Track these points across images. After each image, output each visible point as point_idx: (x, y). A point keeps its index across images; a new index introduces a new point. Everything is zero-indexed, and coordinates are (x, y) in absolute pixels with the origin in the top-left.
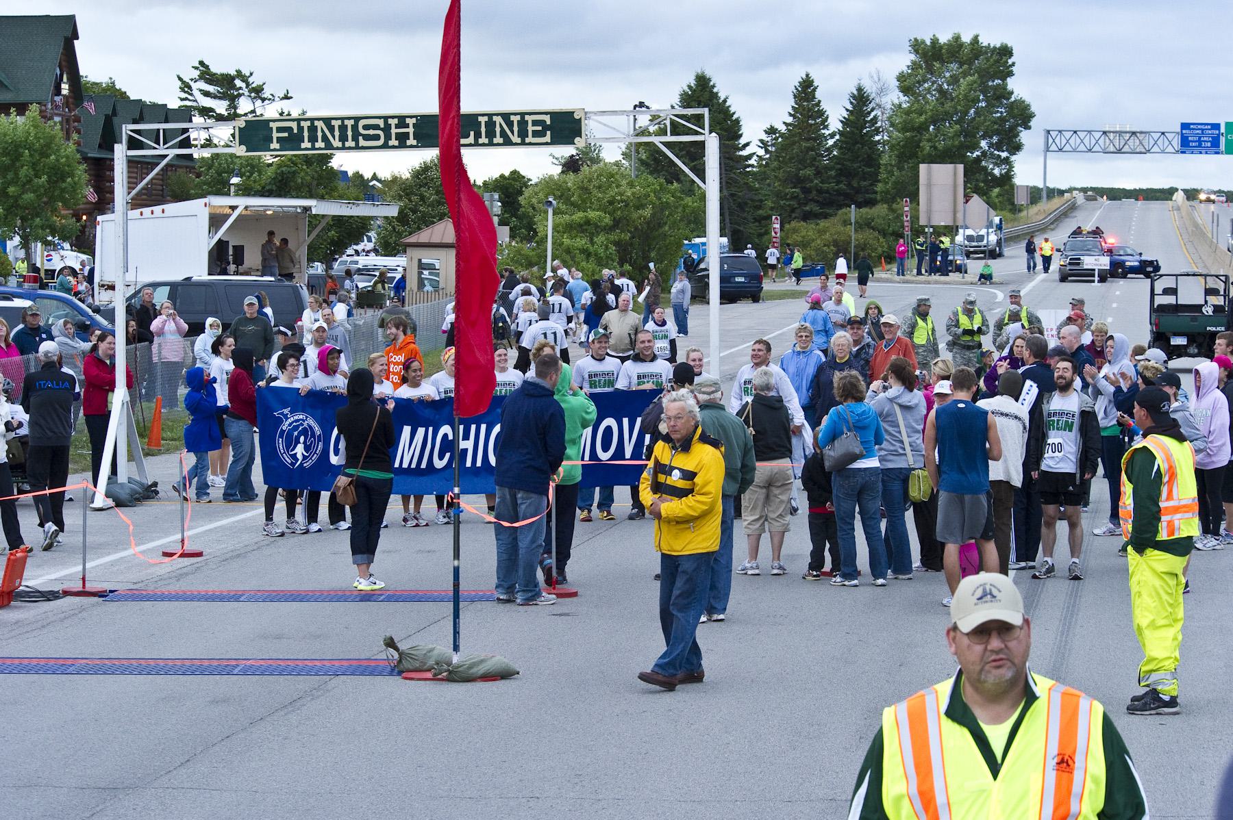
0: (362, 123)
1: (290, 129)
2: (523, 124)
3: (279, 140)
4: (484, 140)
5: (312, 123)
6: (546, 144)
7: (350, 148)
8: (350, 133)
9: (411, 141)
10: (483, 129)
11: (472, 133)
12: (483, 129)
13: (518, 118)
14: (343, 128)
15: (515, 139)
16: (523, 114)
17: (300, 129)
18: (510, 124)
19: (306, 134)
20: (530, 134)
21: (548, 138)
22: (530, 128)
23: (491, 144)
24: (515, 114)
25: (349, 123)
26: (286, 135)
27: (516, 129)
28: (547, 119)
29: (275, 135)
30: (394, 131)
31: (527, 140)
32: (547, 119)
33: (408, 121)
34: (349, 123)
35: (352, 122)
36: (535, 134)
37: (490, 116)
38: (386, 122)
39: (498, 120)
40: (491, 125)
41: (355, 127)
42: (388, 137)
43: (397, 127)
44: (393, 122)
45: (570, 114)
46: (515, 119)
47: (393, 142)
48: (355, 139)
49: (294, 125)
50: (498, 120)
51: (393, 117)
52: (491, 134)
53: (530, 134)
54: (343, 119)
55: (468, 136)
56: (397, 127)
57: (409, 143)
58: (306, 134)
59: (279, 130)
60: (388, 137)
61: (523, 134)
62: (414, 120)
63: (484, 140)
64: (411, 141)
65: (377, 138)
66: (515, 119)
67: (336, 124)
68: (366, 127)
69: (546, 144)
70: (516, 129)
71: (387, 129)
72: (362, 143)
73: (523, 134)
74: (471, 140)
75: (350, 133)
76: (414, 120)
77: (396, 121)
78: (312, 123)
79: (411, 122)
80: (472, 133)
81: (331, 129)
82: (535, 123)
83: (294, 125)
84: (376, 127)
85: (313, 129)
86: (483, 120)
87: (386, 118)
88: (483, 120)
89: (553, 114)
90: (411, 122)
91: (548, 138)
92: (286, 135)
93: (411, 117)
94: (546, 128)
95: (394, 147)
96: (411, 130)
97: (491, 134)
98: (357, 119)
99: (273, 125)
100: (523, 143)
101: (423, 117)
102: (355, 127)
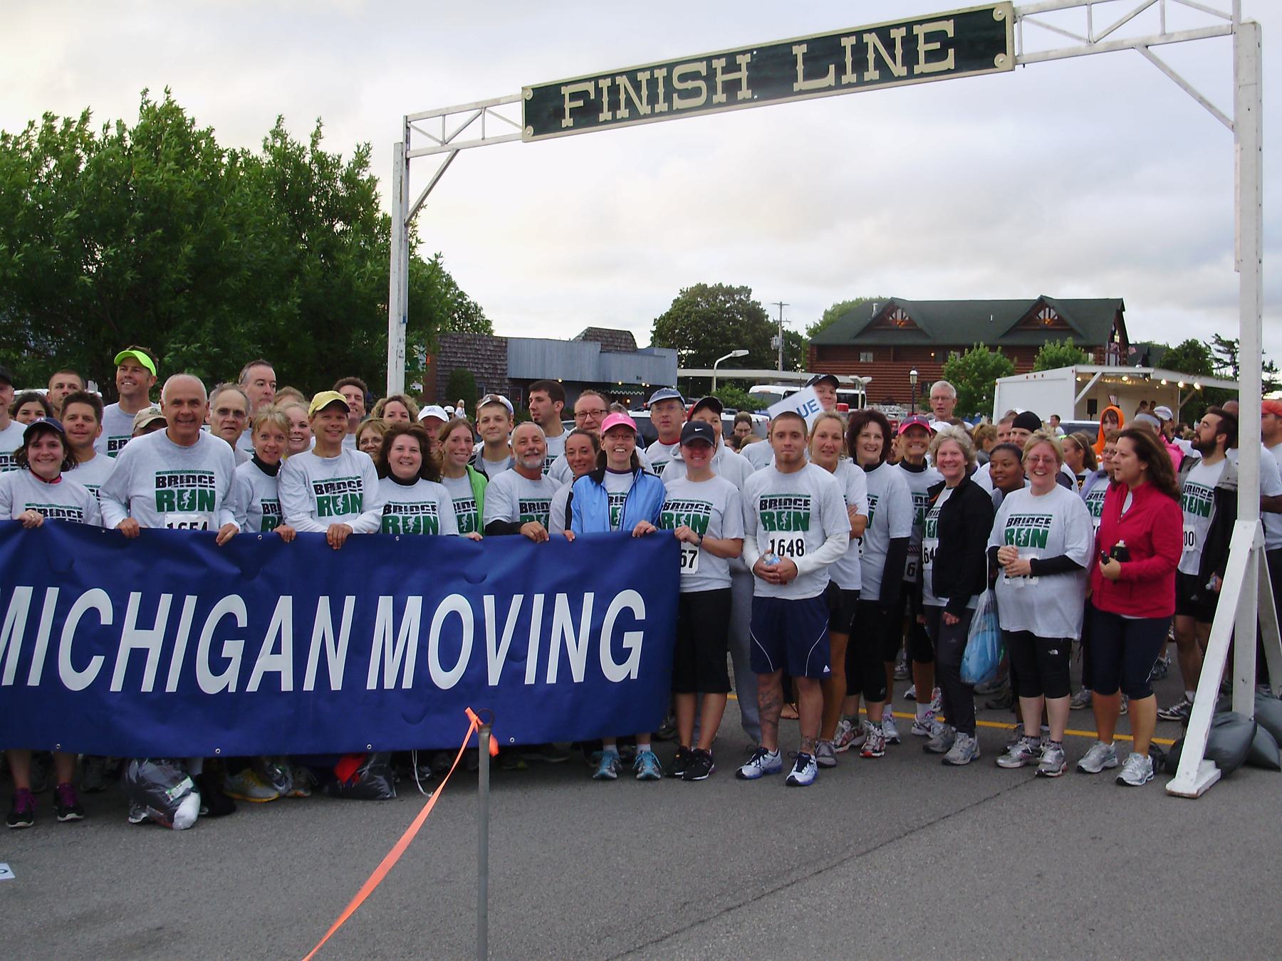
0: (677, 71)
1: (583, 95)
2: (910, 41)
3: (573, 112)
4: (850, 77)
5: (613, 82)
6: (949, 71)
7: (661, 114)
8: (661, 90)
9: (745, 93)
10: (849, 59)
11: (832, 68)
12: (849, 59)
13: (903, 32)
14: (652, 82)
15: (899, 69)
16: (909, 25)
17: (599, 91)
18: (890, 45)
19: (605, 99)
20: (922, 56)
21: (950, 62)
22: (922, 48)
23: (861, 83)
24: (898, 26)
25: (660, 74)
26: (581, 103)
27: (899, 51)
28: (949, 27)
29: (568, 105)
30: (720, 78)
31: (917, 70)
32: (949, 27)
33: (739, 59)
34: (660, 74)
35: (664, 72)
36: (932, 56)
37: (859, 34)
38: (709, 67)
39: (871, 39)
40: (860, 49)
41: (668, 80)
42: (712, 89)
43: (726, 70)
44: (719, 64)
45: (989, 12)
46: (898, 34)
47: (720, 97)
48: (668, 99)
49: (590, 87)
50: (871, 39)
51: (718, 57)
52: (860, 65)
53: (922, 56)
54: (651, 69)
55: (825, 73)
56: (726, 70)
57: (741, 95)
58: (605, 99)
59: (574, 96)
60: (712, 89)
61: (910, 59)
62: (748, 58)
63: (850, 77)
64: (745, 93)
65: (696, 92)
66: (898, 34)
67: (643, 77)
68: (684, 78)
69: (949, 71)
70: (899, 51)
71: (710, 77)
72: (678, 103)
73: (910, 59)
74: (830, 79)
75: (661, 90)
76: (748, 58)
77: (723, 62)
78: (613, 82)
79: (743, 60)
80: (832, 68)
81: (637, 86)
82: (929, 37)
83: (590, 87)
84: (695, 76)
85: (614, 90)
86: (848, 43)
87: (709, 59)
88: (848, 43)
89: (964, 20)
90: (743, 60)
91: (950, 62)
92: (581, 103)
93: (744, 52)
94: (947, 43)
95: (720, 105)
96: (743, 74)
97: (860, 65)
98: (670, 66)
99: (566, 91)
100: (911, 75)
101: (762, 50)
102: (668, 80)
